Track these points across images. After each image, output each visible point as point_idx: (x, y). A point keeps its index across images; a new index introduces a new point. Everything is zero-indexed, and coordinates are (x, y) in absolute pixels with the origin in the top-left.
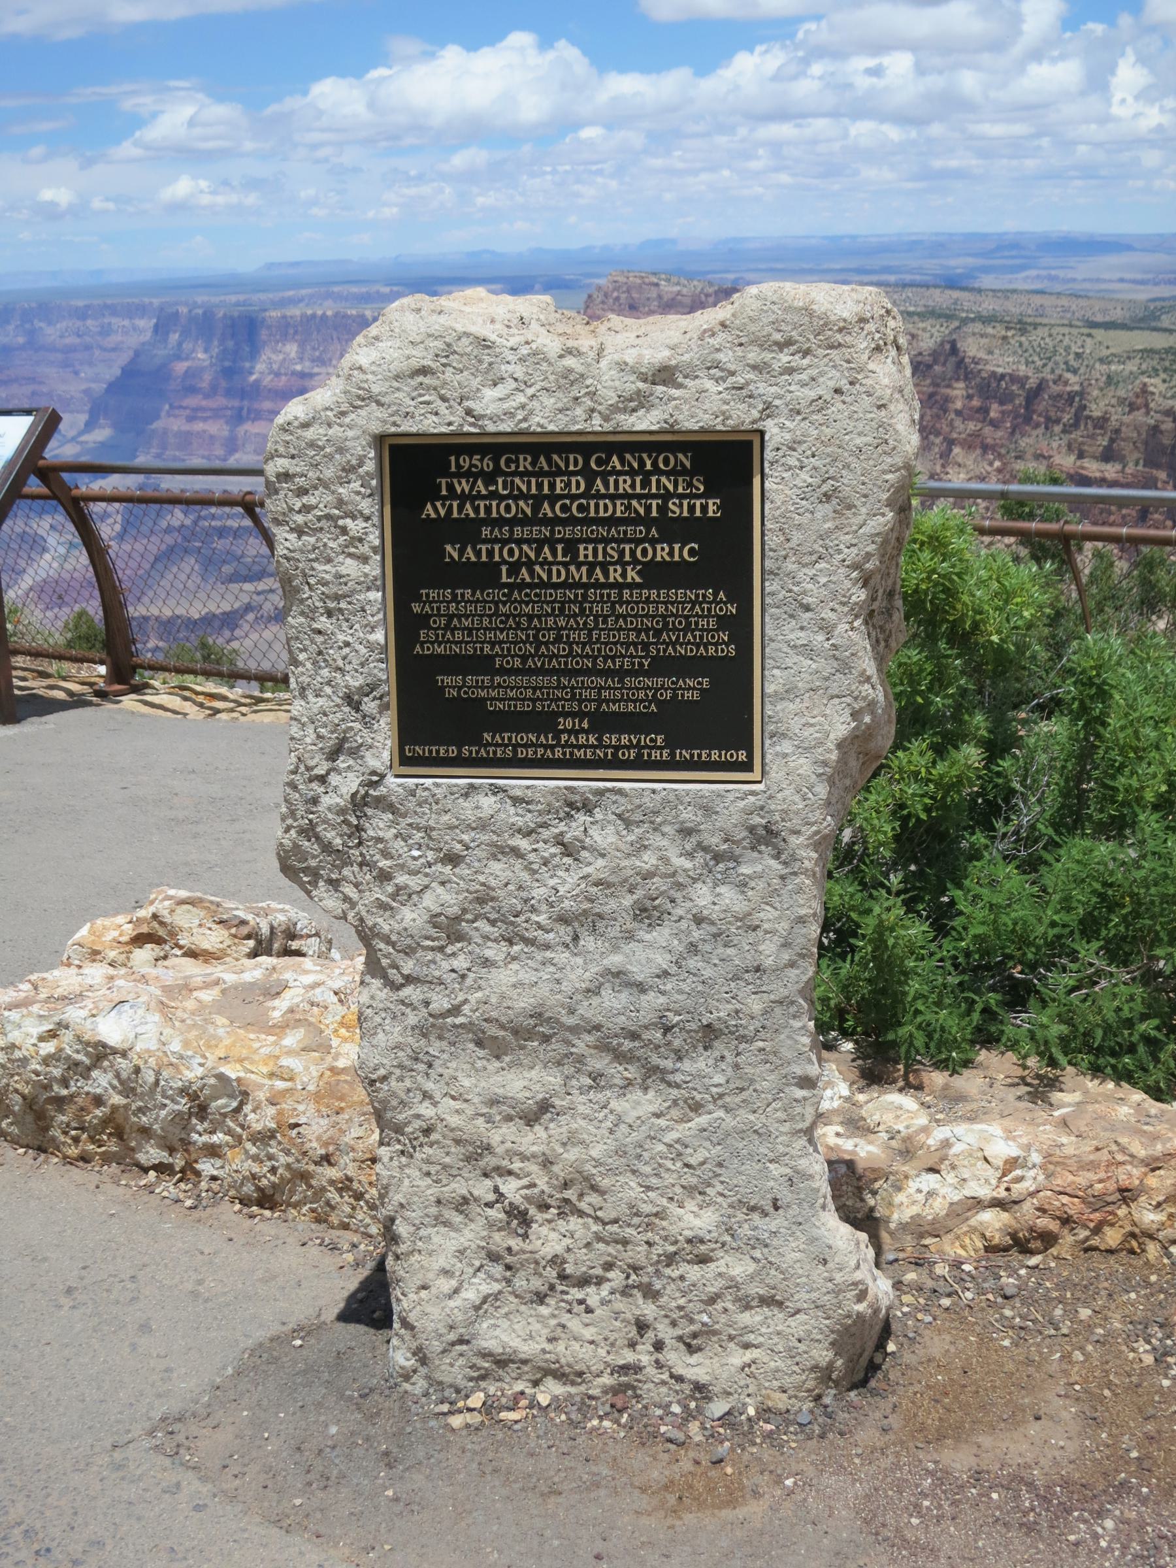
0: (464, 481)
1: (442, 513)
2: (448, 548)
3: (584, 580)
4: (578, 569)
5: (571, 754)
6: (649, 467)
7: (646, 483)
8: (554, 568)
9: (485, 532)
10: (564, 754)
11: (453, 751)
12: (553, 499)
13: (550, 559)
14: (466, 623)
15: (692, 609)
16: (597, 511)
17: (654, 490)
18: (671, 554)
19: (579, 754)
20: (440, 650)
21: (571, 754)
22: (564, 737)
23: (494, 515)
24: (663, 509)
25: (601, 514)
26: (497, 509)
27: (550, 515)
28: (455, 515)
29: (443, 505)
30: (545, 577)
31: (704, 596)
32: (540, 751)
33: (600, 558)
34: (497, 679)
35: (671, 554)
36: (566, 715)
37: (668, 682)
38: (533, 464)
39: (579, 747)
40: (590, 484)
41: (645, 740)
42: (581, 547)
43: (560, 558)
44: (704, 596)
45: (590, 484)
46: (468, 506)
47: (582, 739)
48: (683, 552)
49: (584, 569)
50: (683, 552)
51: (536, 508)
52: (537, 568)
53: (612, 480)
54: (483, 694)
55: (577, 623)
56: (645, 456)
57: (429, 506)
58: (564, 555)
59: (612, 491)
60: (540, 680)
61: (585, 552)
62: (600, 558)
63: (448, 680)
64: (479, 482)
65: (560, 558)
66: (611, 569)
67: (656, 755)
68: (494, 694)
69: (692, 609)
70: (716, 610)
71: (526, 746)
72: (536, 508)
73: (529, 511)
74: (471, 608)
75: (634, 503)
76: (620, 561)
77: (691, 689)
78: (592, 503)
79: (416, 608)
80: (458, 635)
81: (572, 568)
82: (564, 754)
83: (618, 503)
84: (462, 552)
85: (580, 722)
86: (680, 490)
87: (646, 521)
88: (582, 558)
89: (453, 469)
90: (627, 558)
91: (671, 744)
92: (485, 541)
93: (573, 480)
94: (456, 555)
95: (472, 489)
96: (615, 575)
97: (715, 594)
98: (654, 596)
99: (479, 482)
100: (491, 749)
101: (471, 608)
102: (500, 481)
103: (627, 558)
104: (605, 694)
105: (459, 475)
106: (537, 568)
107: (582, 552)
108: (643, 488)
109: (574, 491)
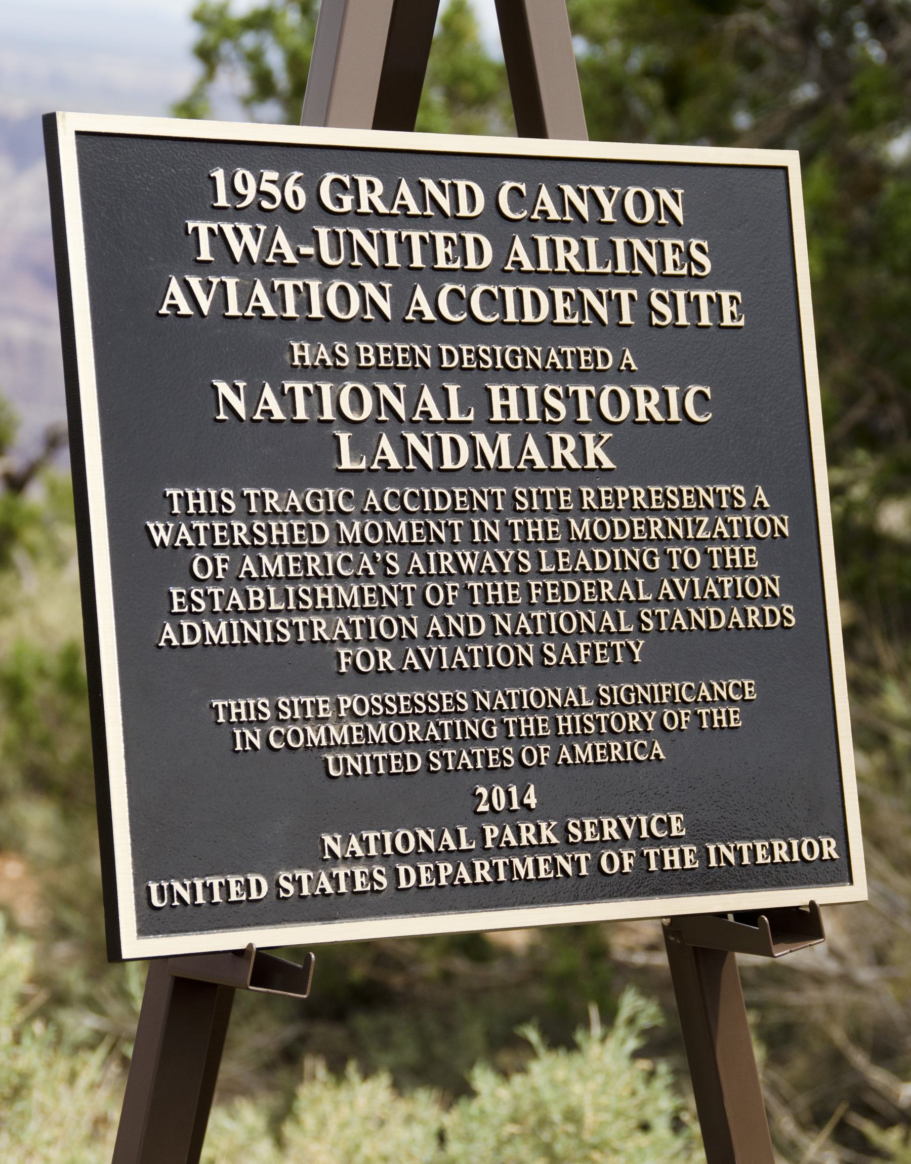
0: (245, 229)
1: (205, 305)
2: (224, 388)
3: (506, 464)
4: (493, 441)
5: (510, 867)
6: (609, 217)
7: (608, 251)
8: (446, 438)
9: (303, 351)
10: (494, 869)
11: (260, 886)
12: (433, 276)
13: (436, 416)
14: (273, 565)
15: (712, 526)
16: (521, 312)
17: (622, 268)
18: (664, 406)
19: (524, 867)
20: (217, 633)
21: (510, 867)
22: (491, 832)
23: (316, 312)
24: (643, 306)
25: (529, 317)
26: (323, 297)
27: (429, 315)
28: (233, 310)
29: (207, 286)
30: (428, 457)
31: (731, 496)
32: (446, 869)
33: (533, 416)
34: (348, 701)
35: (664, 406)
36: (490, 775)
37: (681, 688)
38: (389, 197)
39: (521, 850)
40: (503, 249)
41: (650, 824)
42: (495, 390)
43: (455, 416)
44: (731, 496)
45: (503, 249)
46: (259, 290)
47: (528, 836)
48: (686, 401)
49: (503, 439)
50: (686, 401)
51: (402, 299)
52: (413, 439)
53: (542, 241)
54: (316, 736)
55: (501, 564)
56: (599, 191)
57: (174, 287)
58: (464, 410)
59: (544, 266)
60: (441, 698)
61: (504, 400)
62: (533, 416)
63: (239, 707)
64: (280, 236)
65: (455, 416)
66: (556, 438)
67: (672, 858)
68: (339, 735)
69: (712, 526)
70: (752, 522)
71: (413, 859)
72: (402, 299)
73: (386, 307)
74: (279, 529)
75: (589, 295)
76: (575, 425)
77: (726, 701)
78: (509, 291)
79: (161, 536)
80: (257, 597)
81: (481, 439)
82: (494, 869)
83: (558, 292)
84: (253, 399)
85: (522, 794)
86: (670, 270)
87: (614, 333)
88: (498, 416)
89: (222, 201)
90: (584, 416)
91: (698, 834)
92: (304, 372)
93: (469, 238)
94: (240, 406)
95: (265, 250)
96: (564, 453)
97: (751, 495)
98: (639, 499)
99: (280, 236)
100: (341, 872)
101: (279, 529)
102: (323, 233)
103: (584, 416)
104: (565, 723)
105: (235, 213)
106: (413, 439)
107: (497, 402)
108: (602, 262)
109: (472, 264)
